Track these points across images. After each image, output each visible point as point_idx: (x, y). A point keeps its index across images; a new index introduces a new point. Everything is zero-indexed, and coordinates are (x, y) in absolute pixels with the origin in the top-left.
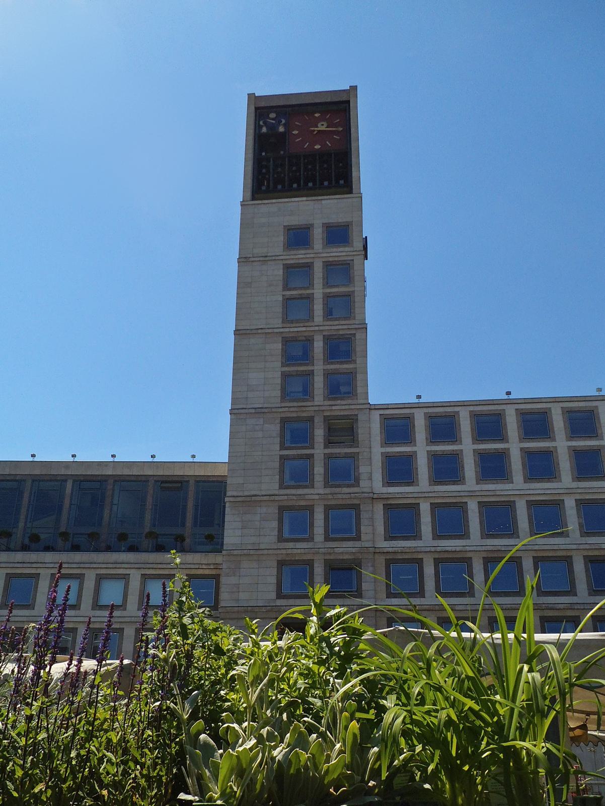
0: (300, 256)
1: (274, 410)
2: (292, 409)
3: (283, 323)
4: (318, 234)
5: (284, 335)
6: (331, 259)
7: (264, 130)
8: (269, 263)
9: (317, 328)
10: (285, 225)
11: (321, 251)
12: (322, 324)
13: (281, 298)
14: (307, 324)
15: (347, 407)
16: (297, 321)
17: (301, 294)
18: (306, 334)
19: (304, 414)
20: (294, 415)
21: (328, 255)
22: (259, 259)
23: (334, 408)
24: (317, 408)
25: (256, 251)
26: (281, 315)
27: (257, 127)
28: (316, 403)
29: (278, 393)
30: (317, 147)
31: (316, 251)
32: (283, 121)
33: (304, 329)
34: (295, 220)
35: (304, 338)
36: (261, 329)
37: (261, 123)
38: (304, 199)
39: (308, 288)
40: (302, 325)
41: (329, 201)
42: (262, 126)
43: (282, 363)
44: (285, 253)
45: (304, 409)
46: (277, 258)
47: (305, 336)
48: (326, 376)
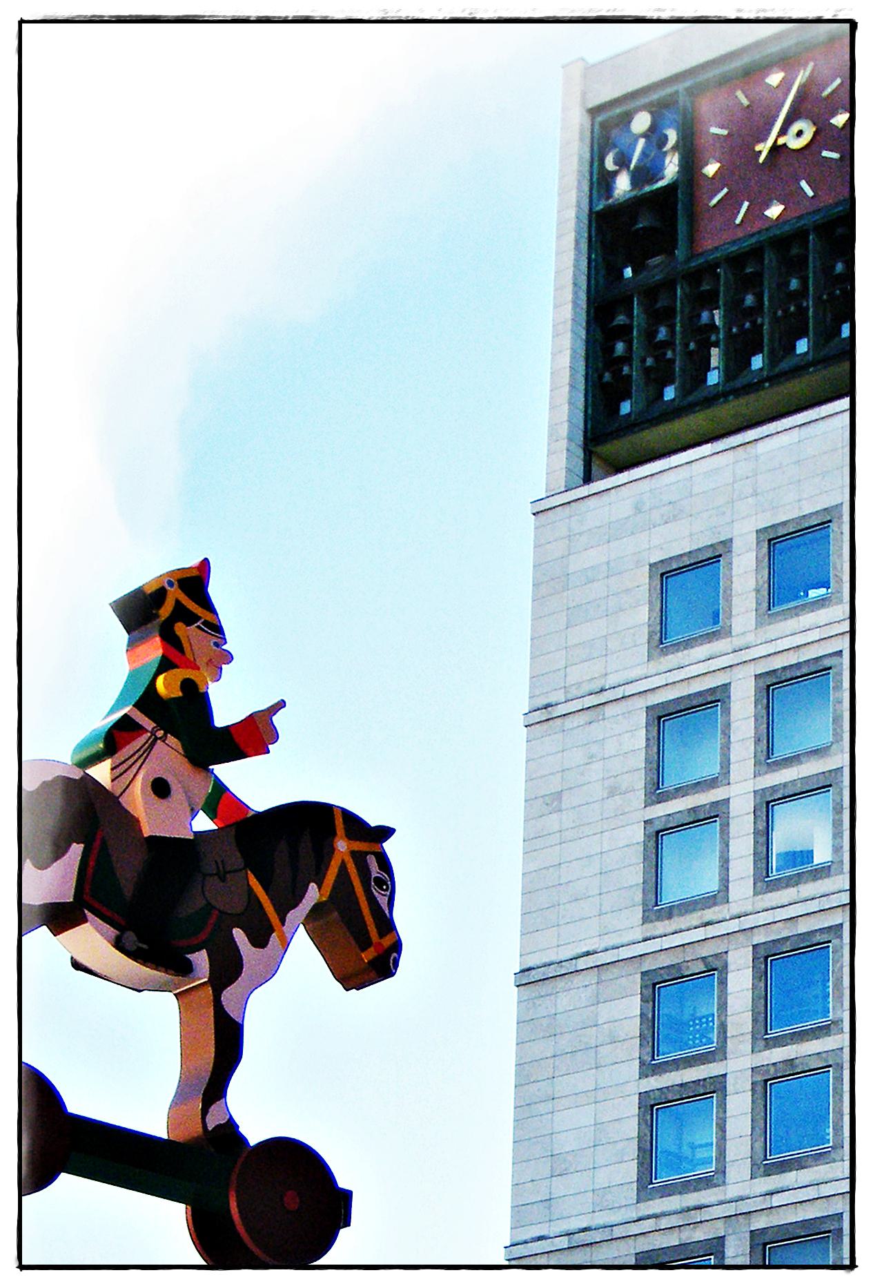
0: (691, 669)
1: (618, 1232)
2: (664, 1222)
3: (645, 920)
4: (745, 573)
5: (648, 965)
6: (778, 663)
7: (623, 184)
8: (610, 710)
9: (734, 926)
10: (652, 561)
11: (750, 638)
12: (749, 909)
13: (640, 836)
14: (709, 915)
15: (811, 1193)
16: (688, 906)
17: (694, 810)
18: (705, 951)
19: (699, 1235)
20: (673, 1240)
21: (771, 649)
22: (577, 705)
23: (777, 1200)
24: (730, 1209)
25: (575, 675)
26: (639, 897)
27: (602, 181)
28: (732, 1191)
29: (630, 1171)
30: (774, 211)
31: (737, 642)
32: (672, 136)
33: (699, 934)
34: (680, 540)
35: (700, 967)
36: (588, 954)
37: (610, 164)
38: (707, 449)
39: (712, 783)
40: (694, 918)
41: (784, 439)
42: (615, 173)
43: (642, 1063)
44: (653, 667)
45: (698, 1216)
46: (629, 690)
47: (704, 959)
48: (759, 1089)
